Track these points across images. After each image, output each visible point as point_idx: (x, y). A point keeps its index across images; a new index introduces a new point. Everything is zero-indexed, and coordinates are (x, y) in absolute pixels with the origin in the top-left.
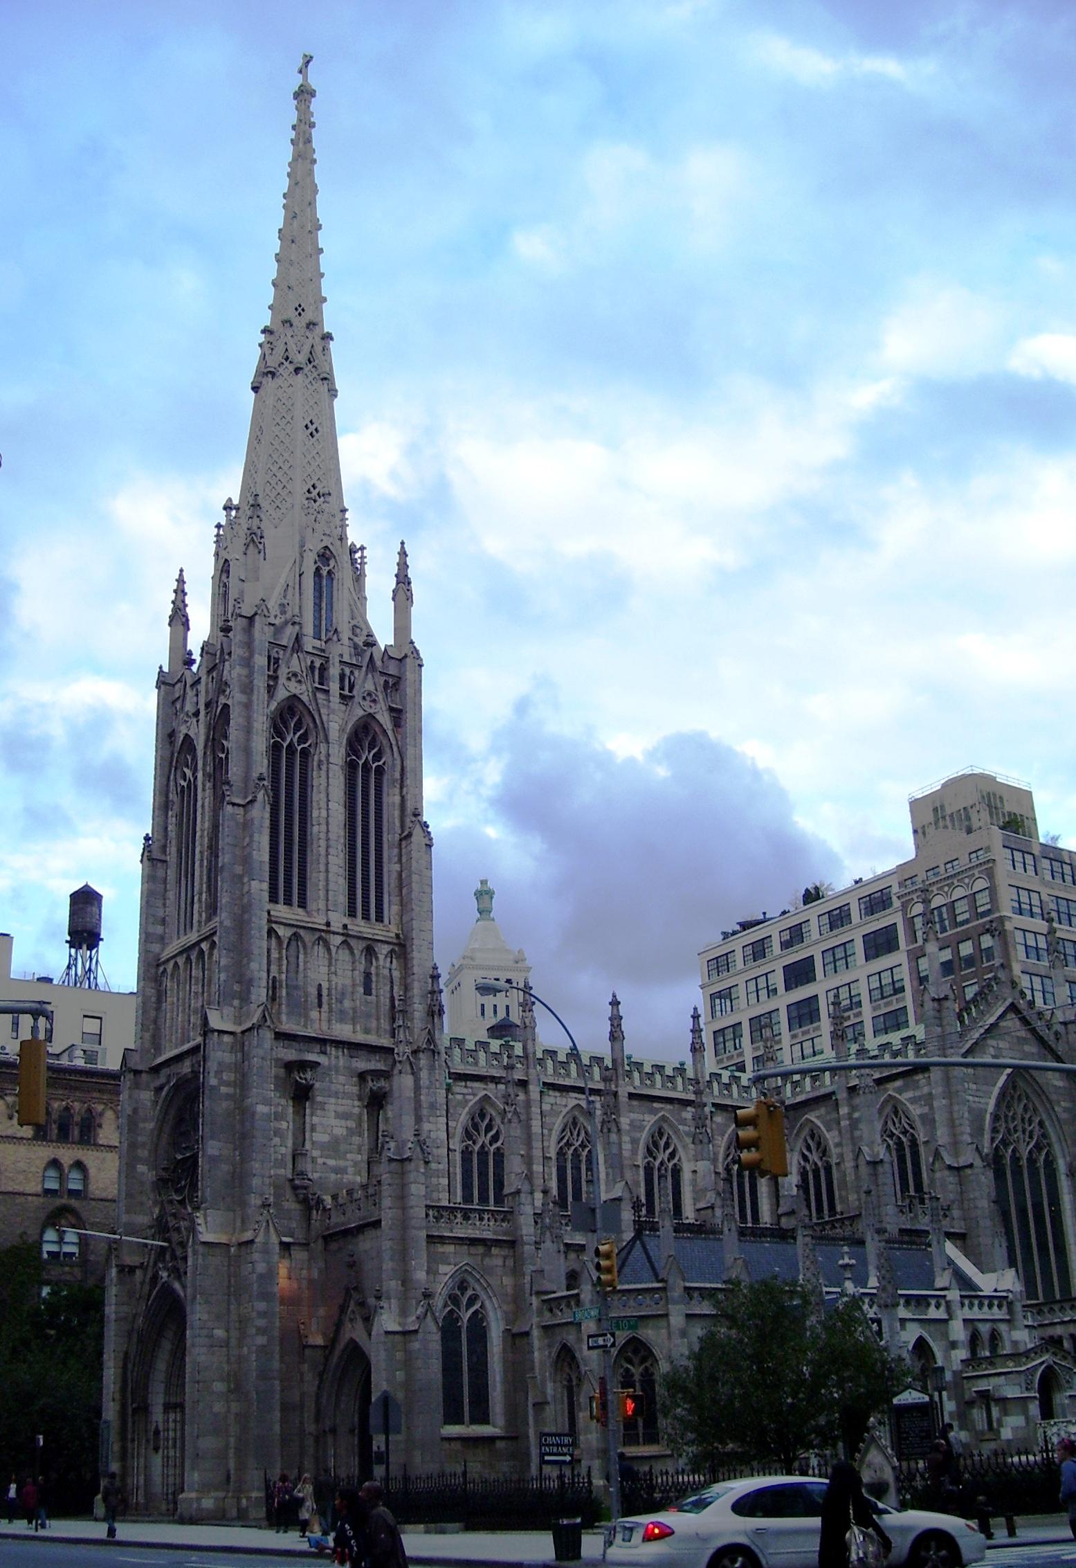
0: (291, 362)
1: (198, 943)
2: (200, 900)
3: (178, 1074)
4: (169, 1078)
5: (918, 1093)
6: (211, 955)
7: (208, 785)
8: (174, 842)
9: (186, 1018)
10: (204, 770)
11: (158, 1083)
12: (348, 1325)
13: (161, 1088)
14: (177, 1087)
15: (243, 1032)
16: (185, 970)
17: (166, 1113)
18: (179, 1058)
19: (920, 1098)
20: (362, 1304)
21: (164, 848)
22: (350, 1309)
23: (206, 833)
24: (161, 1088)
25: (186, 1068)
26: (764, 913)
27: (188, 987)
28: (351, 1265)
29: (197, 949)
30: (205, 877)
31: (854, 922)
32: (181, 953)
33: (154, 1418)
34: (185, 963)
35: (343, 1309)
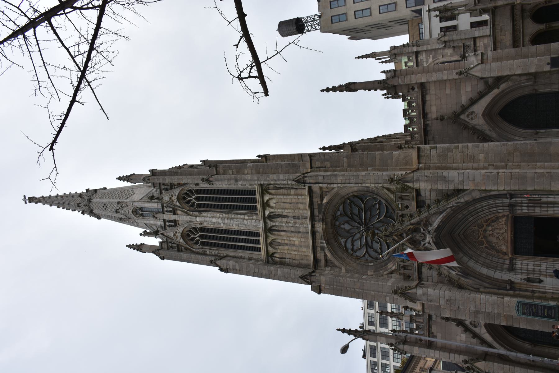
0: (92, 195)
1: (265, 218)
2: (247, 220)
3: (321, 239)
4: (322, 248)
5: (425, 60)
6: (272, 207)
7: (203, 214)
8: (220, 252)
9: (297, 235)
10: (196, 216)
11: (323, 263)
12: (473, 122)
13: (326, 260)
14: (328, 243)
15: (311, 167)
16: (274, 235)
17: (340, 258)
18: (314, 233)
19: (427, 59)
20: (464, 109)
21: (219, 256)
22: (467, 119)
23: (221, 216)
24: (326, 260)
25: (319, 227)
26: (362, 350)
27: (283, 233)
28: (442, 118)
29: (268, 221)
30: (239, 216)
31: (375, 329)
32: (266, 237)
33: (517, 281)
34: (271, 234)
35: (465, 126)
